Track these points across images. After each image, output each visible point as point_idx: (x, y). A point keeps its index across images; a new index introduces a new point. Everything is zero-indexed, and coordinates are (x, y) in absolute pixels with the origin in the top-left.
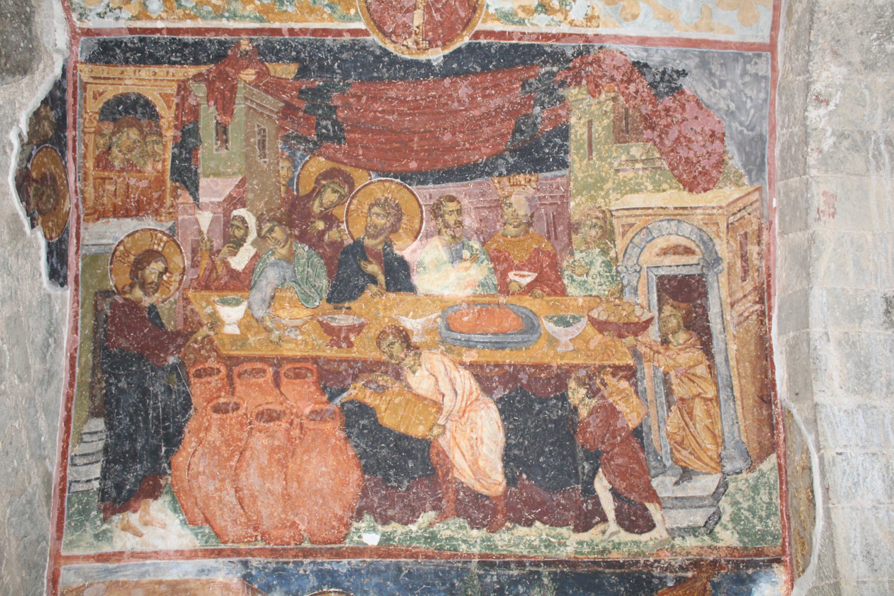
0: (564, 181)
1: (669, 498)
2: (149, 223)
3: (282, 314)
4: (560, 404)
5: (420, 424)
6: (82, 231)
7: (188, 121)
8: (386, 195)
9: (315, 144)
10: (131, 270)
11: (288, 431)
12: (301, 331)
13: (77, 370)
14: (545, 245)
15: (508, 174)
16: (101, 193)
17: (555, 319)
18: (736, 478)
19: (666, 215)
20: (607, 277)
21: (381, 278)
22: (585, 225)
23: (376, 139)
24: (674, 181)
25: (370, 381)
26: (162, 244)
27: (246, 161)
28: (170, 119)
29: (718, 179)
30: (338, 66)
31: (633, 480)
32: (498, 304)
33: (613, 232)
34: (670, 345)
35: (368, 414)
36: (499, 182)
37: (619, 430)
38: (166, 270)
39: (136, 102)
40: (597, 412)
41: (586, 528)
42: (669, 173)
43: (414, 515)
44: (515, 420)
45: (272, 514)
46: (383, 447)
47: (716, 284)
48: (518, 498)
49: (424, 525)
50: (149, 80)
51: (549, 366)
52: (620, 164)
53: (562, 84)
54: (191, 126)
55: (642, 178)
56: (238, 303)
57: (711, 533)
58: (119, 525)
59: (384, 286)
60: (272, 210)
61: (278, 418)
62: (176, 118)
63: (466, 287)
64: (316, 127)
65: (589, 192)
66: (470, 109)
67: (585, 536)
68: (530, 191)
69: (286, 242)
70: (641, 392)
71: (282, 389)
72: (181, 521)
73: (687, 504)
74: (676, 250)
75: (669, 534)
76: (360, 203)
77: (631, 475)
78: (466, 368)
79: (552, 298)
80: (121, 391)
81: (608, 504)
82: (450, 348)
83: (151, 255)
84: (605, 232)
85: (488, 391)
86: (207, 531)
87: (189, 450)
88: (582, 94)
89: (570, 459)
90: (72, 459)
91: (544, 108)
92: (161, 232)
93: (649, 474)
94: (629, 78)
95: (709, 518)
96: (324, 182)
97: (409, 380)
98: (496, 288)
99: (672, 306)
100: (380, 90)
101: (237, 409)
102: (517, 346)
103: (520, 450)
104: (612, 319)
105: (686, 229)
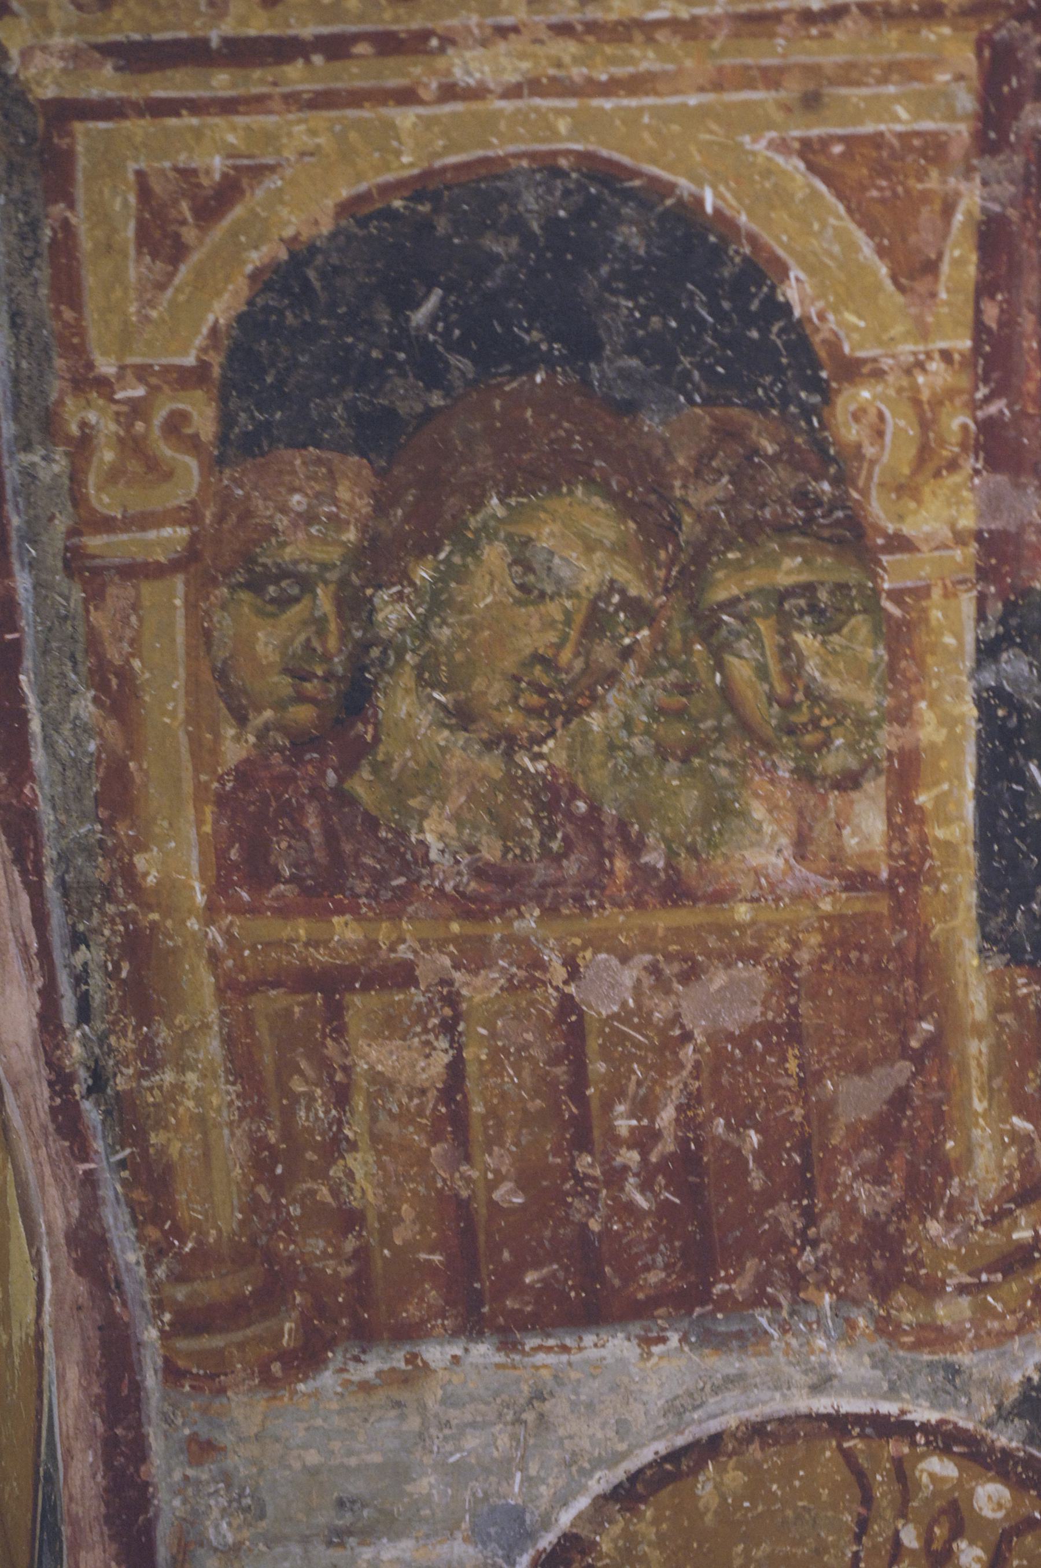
6: (163, 1466)
16: (314, 1114)
28: (936, 377)
92: (945, 1439)
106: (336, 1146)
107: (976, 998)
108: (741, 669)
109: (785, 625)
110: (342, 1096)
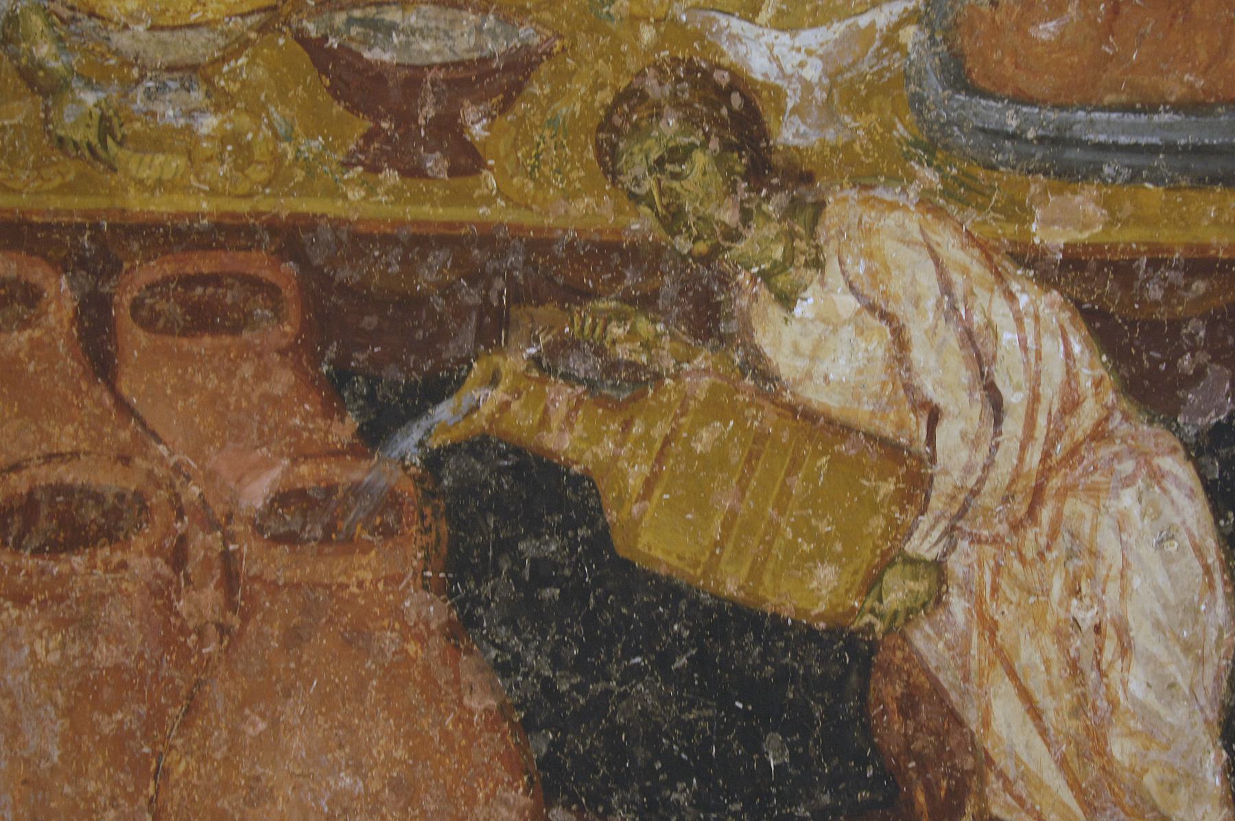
5: (821, 555)
12: (211, 90)
25: (563, 346)
46: (638, 673)
61: (111, 533)
71: (124, 387)
78: (1045, 281)
82: (965, 180)
97: (763, 339)
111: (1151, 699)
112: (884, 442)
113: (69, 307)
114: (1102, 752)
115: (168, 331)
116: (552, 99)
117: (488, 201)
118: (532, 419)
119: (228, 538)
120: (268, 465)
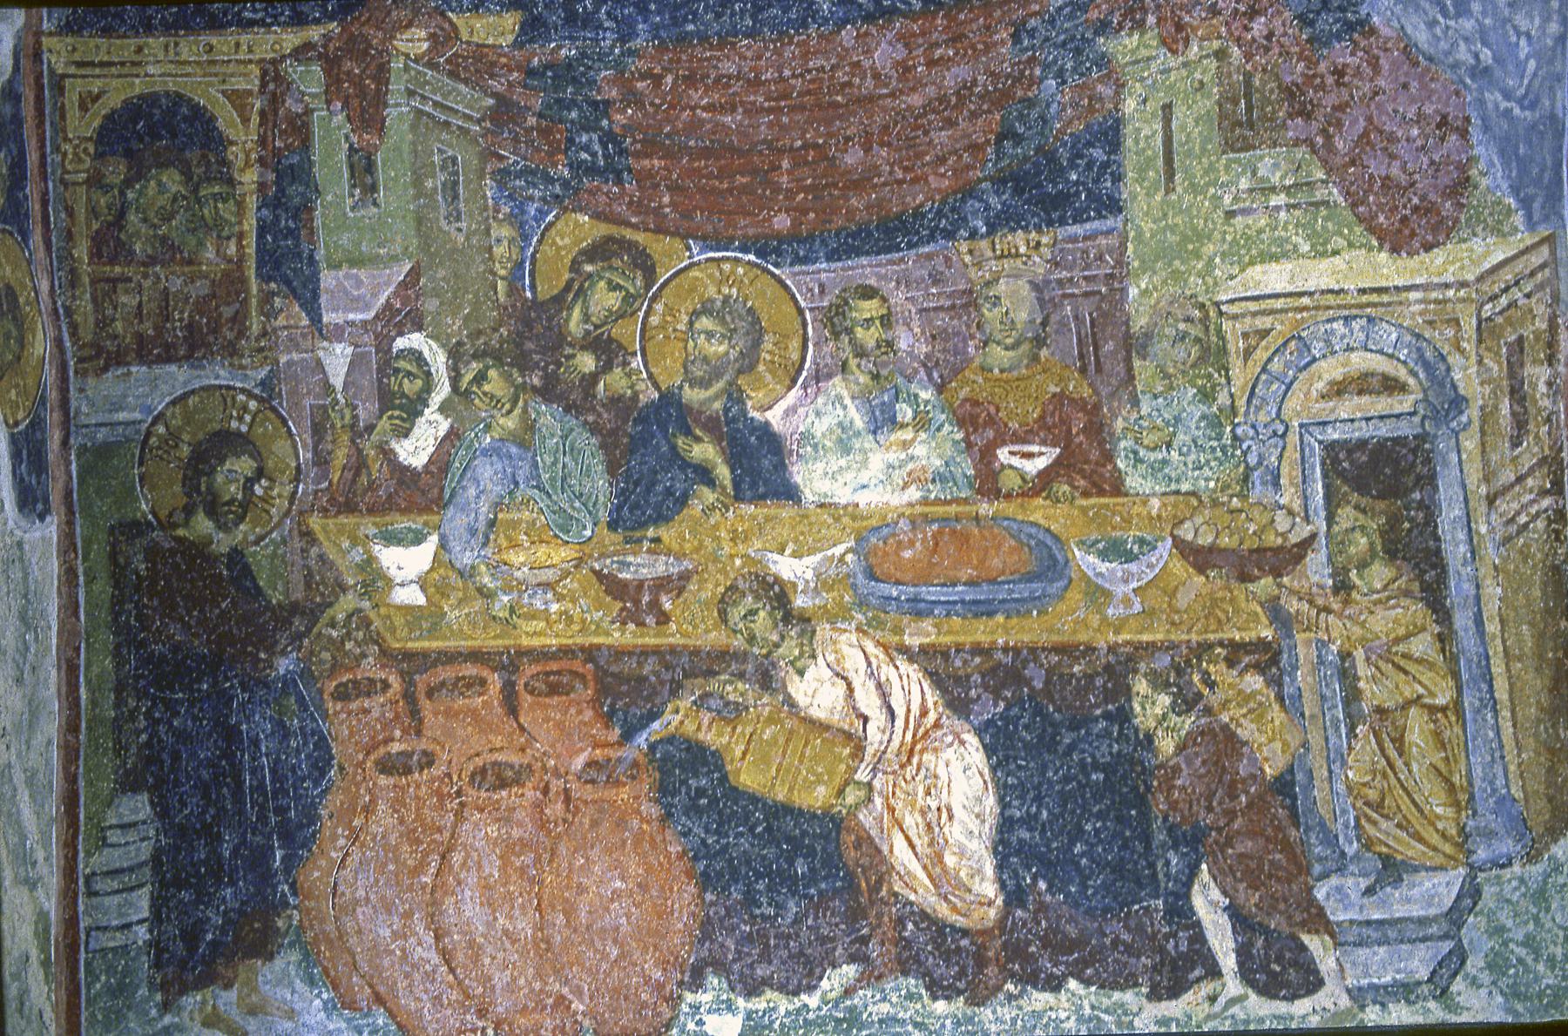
0: (1113, 241)
1: (1352, 922)
2: (218, 374)
3: (517, 558)
4: (1116, 728)
5: (819, 782)
7: (287, 147)
8: (726, 291)
9: (566, 184)
10: (185, 476)
11: (538, 806)
13: (83, 694)
14: (1079, 388)
15: (989, 233)
16: (109, 312)
17: (1100, 546)
18: (1498, 877)
19: (1339, 307)
20: (1213, 449)
21: (723, 472)
22: (1162, 336)
23: (699, 169)
24: (1358, 230)
25: (706, 696)
26: (248, 418)
27: (419, 230)
28: (249, 145)
29: (1456, 221)
30: (608, 14)
31: (1275, 887)
32: (977, 518)
33: (1223, 351)
34: (1354, 594)
35: (705, 763)
36: (971, 252)
37: (1244, 781)
38: (260, 473)
39: (172, 112)
40: (1195, 743)
41: (1174, 992)
42: (1348, 214)
43: (810, 974)
44: (1020, 767)
45: (514, 979)
46: (742, 834)
47: (1454, 457)
48: (1030, 931)
49: (833, 995)
50: (198, 63)
51: (1090, 649)
52: (1236, 199)
53: (1103, 27)
54: (295, 159)
55: (1285, 229)
56: (418, 539)
57: (1443, 995)
58: (196, 1015)
59: (730, 490)
60: (480, 333)
62: (262, 141)
63: (905, 487)
64: (567, 149)
65: (1170, 265)
66: (902, 92)
67: (1172, 1008)
68: (1039, 266)
69: (515, 402)
70: (1291, 697)
72: (325, 1003)
73: (1392, 934)
74: (1362, 384)
75: (1352, 998)
76: (670, 310)
77: (1270, 876)
78: (911, 660)
79: (1093, 501)
80: (182, 736)
81: (1222, 943)
83: (224, 443)
84: (1205, 351)
85: (959, 706)
86: (380, 1022)
87: (334, 855)
88: (1147, 46)
89: (1140, 848)
90: (88, 879)
91: (1064, 82)
92: (243, 390)
93: (1308, 873)
94: (1252, 7)
95: (1440, 964)
96: (589, 268)
98: (971, 486)
99: (1357, 507)
100: (700, 60)
101: (430, 764)
102: (1016, 609)
103: (1031, 830)
104: (1225, 541)
105: (1388, 335)
106: (113, 320)
107: (254, 290)
108: (206, 211)
109: (216, 201)
110: (115, 308)
111: (963, 839)
112: (844, 732)
113: (498, 686)
114: (941, 862)
115: (539, 695)
116: (699, 590)
117: (673, 635)
118: (694, 727)
119: (566, 782)
120: (582, 750)
